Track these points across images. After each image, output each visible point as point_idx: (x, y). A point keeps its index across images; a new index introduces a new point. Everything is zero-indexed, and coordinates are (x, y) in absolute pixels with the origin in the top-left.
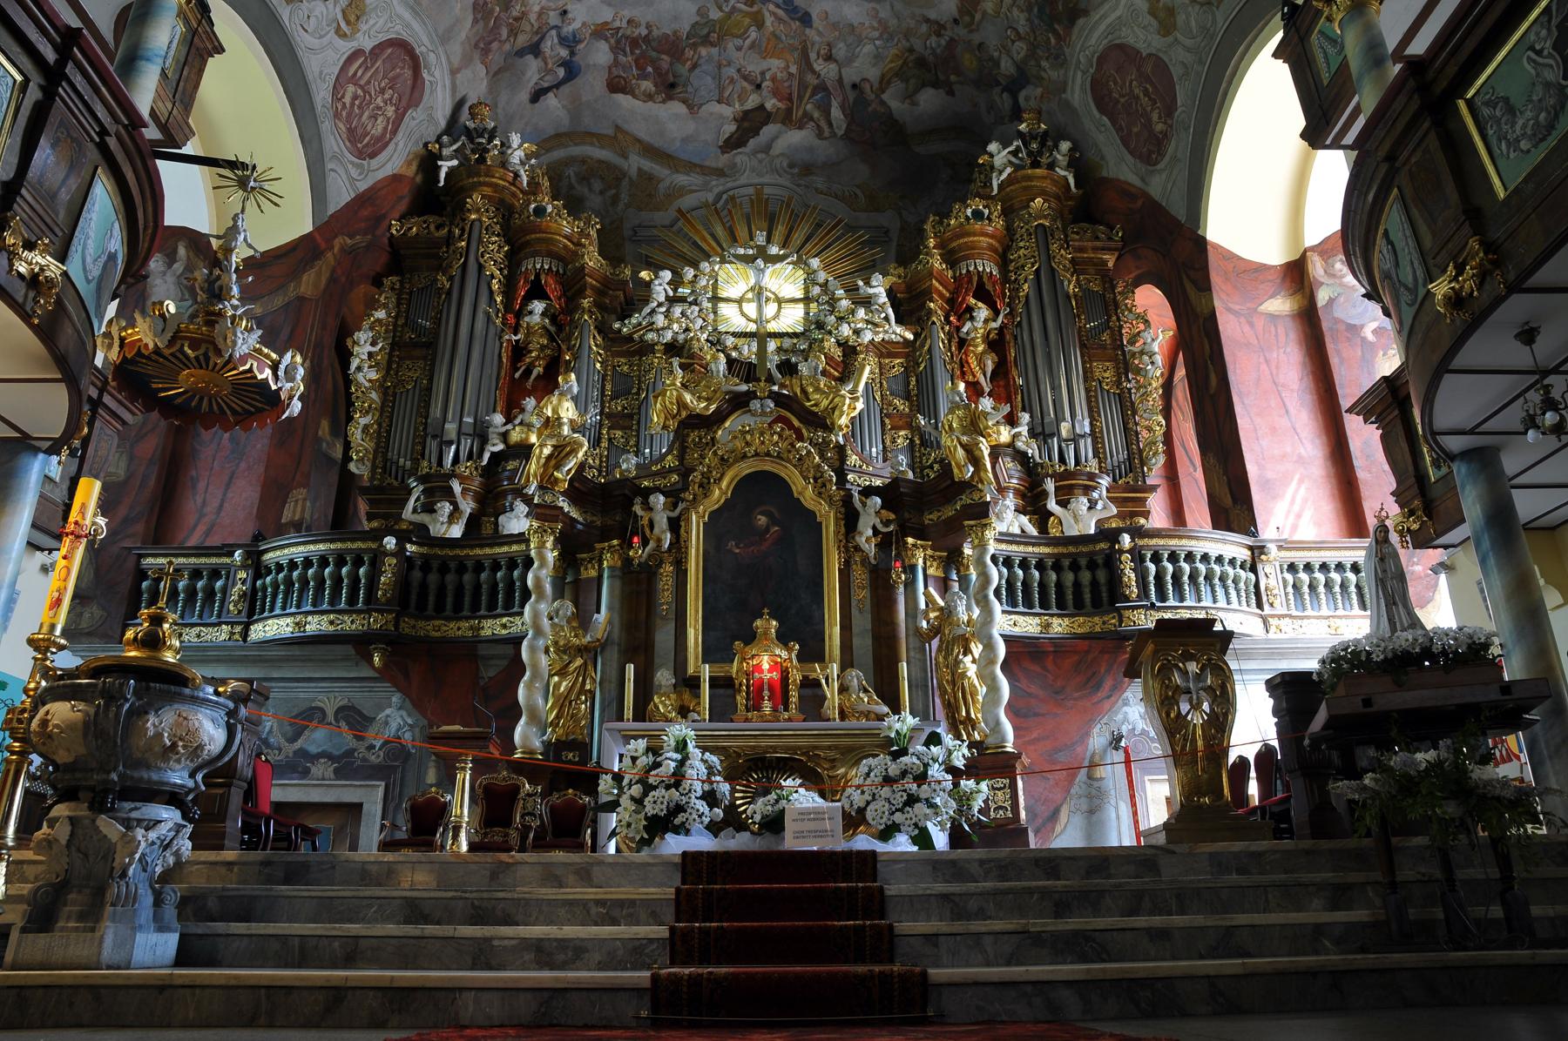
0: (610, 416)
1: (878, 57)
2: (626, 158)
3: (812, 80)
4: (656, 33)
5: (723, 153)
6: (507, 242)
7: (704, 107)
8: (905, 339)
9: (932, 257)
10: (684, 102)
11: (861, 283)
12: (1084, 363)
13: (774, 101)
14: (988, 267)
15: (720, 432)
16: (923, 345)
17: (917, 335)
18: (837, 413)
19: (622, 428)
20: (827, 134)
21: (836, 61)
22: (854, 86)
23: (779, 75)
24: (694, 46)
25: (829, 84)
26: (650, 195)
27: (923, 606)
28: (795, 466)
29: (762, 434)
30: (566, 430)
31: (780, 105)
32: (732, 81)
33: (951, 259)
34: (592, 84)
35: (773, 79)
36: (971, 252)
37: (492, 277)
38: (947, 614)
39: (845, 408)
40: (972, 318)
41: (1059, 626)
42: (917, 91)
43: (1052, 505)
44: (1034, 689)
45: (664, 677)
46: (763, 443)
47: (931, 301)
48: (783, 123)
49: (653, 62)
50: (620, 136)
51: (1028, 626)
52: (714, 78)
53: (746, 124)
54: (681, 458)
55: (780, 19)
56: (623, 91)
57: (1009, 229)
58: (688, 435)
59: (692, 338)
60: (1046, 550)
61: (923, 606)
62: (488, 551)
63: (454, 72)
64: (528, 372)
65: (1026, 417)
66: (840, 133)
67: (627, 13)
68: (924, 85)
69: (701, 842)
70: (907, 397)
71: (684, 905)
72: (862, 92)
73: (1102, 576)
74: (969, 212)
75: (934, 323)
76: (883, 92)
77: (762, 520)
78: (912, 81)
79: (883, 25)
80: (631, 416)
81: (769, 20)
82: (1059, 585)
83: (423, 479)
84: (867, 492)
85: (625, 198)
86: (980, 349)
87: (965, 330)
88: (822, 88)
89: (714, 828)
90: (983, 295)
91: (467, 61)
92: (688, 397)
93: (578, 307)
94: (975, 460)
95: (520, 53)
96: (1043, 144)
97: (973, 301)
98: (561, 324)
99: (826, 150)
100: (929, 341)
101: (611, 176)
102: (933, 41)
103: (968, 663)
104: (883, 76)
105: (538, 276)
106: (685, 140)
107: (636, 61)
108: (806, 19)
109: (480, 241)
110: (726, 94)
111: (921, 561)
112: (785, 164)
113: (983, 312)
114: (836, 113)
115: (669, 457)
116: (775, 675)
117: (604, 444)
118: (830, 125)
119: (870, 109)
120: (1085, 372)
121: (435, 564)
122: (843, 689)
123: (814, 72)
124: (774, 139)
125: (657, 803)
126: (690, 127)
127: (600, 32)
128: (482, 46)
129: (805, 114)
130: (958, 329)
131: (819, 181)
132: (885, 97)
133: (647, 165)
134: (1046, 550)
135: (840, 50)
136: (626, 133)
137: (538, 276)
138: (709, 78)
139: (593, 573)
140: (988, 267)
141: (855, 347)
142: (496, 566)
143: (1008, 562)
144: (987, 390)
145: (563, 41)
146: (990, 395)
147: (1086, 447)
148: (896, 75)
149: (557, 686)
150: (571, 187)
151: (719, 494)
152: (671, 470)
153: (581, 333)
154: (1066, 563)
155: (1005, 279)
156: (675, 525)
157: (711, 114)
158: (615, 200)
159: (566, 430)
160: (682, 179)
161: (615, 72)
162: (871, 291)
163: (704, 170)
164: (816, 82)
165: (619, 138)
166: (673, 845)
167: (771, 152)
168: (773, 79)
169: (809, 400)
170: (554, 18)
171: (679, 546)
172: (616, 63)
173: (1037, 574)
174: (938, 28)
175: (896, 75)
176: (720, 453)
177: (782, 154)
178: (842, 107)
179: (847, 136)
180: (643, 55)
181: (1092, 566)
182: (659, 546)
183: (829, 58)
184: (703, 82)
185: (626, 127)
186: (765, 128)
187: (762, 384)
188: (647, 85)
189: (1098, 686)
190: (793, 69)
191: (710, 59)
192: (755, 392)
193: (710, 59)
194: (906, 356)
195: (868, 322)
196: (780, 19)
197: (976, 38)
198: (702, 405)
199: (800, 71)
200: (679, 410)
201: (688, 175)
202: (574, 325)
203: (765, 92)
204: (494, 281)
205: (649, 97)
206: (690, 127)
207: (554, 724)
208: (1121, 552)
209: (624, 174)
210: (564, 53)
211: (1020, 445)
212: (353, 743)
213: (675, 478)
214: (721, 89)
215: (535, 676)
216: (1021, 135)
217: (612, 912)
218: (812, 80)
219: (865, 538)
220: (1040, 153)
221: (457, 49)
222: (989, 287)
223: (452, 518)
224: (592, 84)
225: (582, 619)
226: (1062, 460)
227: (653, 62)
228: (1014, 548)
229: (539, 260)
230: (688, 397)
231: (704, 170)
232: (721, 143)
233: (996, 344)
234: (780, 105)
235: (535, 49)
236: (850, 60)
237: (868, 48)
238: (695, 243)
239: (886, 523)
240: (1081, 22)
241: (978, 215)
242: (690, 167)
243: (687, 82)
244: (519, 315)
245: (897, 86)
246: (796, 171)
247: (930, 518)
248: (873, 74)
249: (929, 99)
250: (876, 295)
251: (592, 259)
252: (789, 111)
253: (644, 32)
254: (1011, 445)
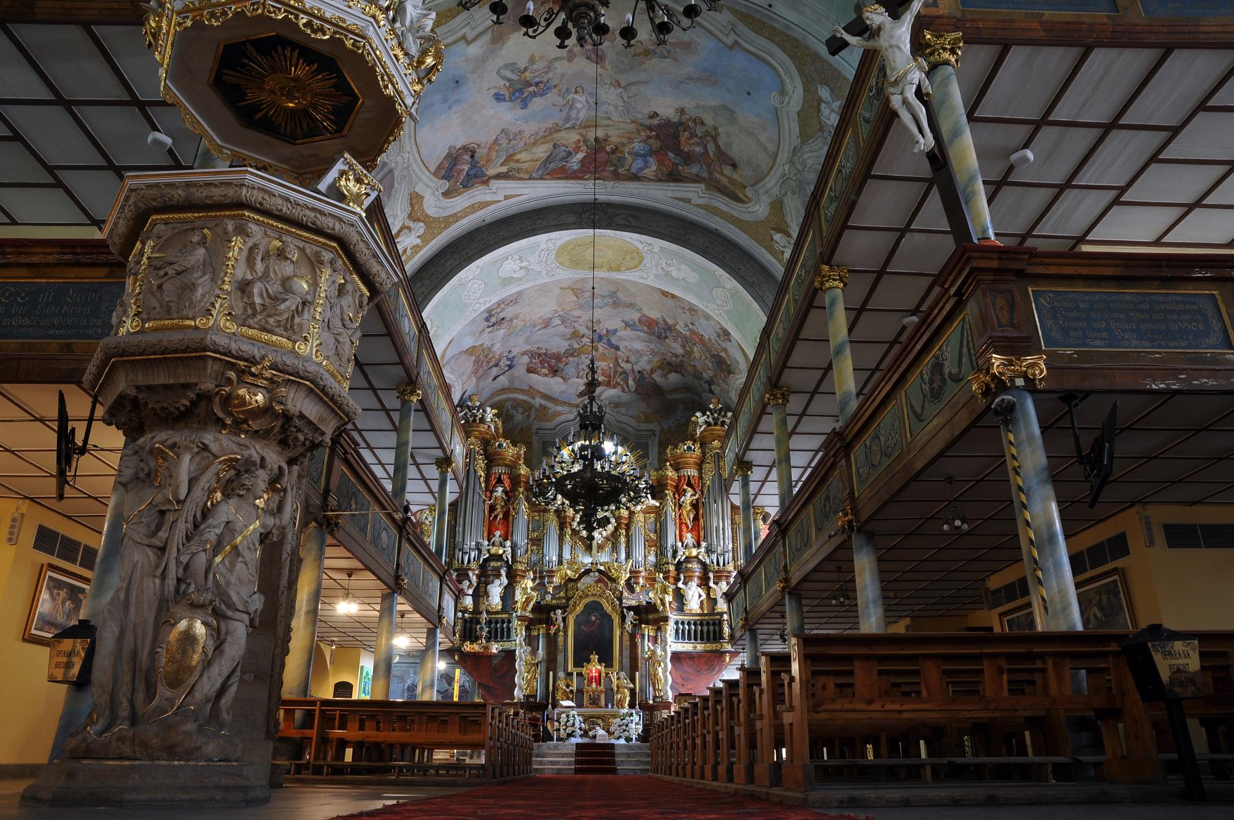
0: (532, 540)
1: (650, 362)
2: (534, 399)
3: (620, 370)
4: (549, 352)
6: (487, 458)
8: (656, 507)
12: (732, 515)
14: (692, 472)
16: (663, 508)
17: (661, 504)
19: (537, 545)
20: (626, 389)
22: (639, 372)
24: (567, 357)
25: (628, 371)
26: (545, 415)
27: (647, 650)
30: (529, 591)
32: (583, 370)
33: (677, 468)
34: (520, 370)
35: (602, 369)
36: (686, 465)
37: (481, 476)
38: (654, 652)
40: (685, 495)
41: (700, 647)
42: (668, 374)
43: (711, 584)
44: (689, 670)
45: (561, 674)
49: (548, 362)
50: (531, 390)
51: (687, 647)
54: (566, 593)
55: (605, 348)
56: (534, 372)
57: (704, 454)
60: (698, 618)
61: (647, 650)
62: (493, 616)
63: (463, 384)
64: (496, 517)
65: (704, 544)
67: (537, 346)
68: (671, 372)
69: (579, 740)
70: (656, 532)
71: (577, 754)
72: (643, 374)
73: (717, 628)
74: (685, 447)
77: (594, 618)
78: (666, 370)
79: (653, 352)
80: (540, 540)
81: (600, 349)
82: (702, 631)
83: (456, 570)
84: (630, 608)
85: (533, 416)
86: (689, 508)
87: (682, 500)
88: (625, 372)
89: (581, 736)
90: (689, 485)
91: (469, 378)
92: (569, 572)
93: (517, 490)
94: (663, 604)
95: (490, 368)
96: (719, 414)
97: (686, 487)
98: (510, 496)
99: (626, 397)
101: (527, 407)
102: (674, 359)
103: (660, 670)
105: (500, 476)
106: (561, 392)
107: (540, 362)
108: (617, 348)
109: (475, 459)
111: (647, 633)
112: (607, 403)
113: (690, 491)
114: (631, 382)
116: (597, 674)
117: (529, 552)
118: (628, 387)
120: (732, 520)
121: (474, 620)
122: (618, 678)
125: (569, 730)
126: (564, 387)
127: (524, 353)
128: (475, 372)
129: (617, 382)
130: (679, 500)
131: (623, 410)
132: (653, 376)
133: (543, 402)
134: (698, 618)
135: (633, 359)
136: (534, 389)
137: (500, 476)
139: (536, 634)
140: (692, 472)
142: (497, 622)
143: (683, 623)
144: (690, 527)
145: (508, 359)
146: (691, 532)
147: (729, 556)
148: (658, 368)
149: (527, 676)
150: (508, 411)
151: (579, 609)
152: (563, 598)
153: (519, 503)
154: (705, 623)
155: (701, 478)
156: (564, 619)
158: (528, 417)
159: (529, 591)
160: (559, 408)
161: (530, 365)
163: (570, 405)
165: (531, 391)
166: (574, 741)
168: (602, 369)
170: (505, 354)
171: (565, 627)
172: (531, 362)
173: (693, 627)
174: (677, 356)
175: (658, 368)
178: (634, 380)
179: (636, 391)
180: (543, 359)
181: (714, 624)
182: (559, 628)
183: (628, 362)
184: (570, 370)
185: (534, 386)
188: (545, 371)
189: (713, 669)
190: (611, 366)
191: (573, 362)
193: (573, 362)
194: (656, 513)
196: (605, 348)
197: (693, 363)
199: (614, 367)
202: (516, 498)
204: (482, 478)
205: (546, 375)
206: (564, 387)
207: (526, 689)
208: (724, 620)
209: (533, 406)
210: (509, 363)
211: (700, 557)
212: (448, 687)
213: (564, 601)
214: (578, 373)
215: (520, 674)
216: (710, 410)
217: (564, 755)
218: (620, 370)
219: (628, 626)
220: (718, 419)
221: (465, 377)
222: (693, 482)
223: (469, 587)
224: (520, 370)
225: (534, 652)
226: (718, 564)
227: (548, 362)
228: (686, 617)
229: (500, 468)
230: (568, 572)
231: (570, 405)
233: (695, 506)
235: (496, 365)
236: (637, 363)
237: (645, 358)
239: (635, 620)
240: (732, 375)
241: (689, 448)
242: (564, 403)
243: (563, 370)
244: (492, 492)
245: (659, 372)
247: (651, 616)
248: (648, 368)
249: (673, 377)
251: (523, 470)
252: (609, 381)
253: (544, 351)
254: (696, 557)
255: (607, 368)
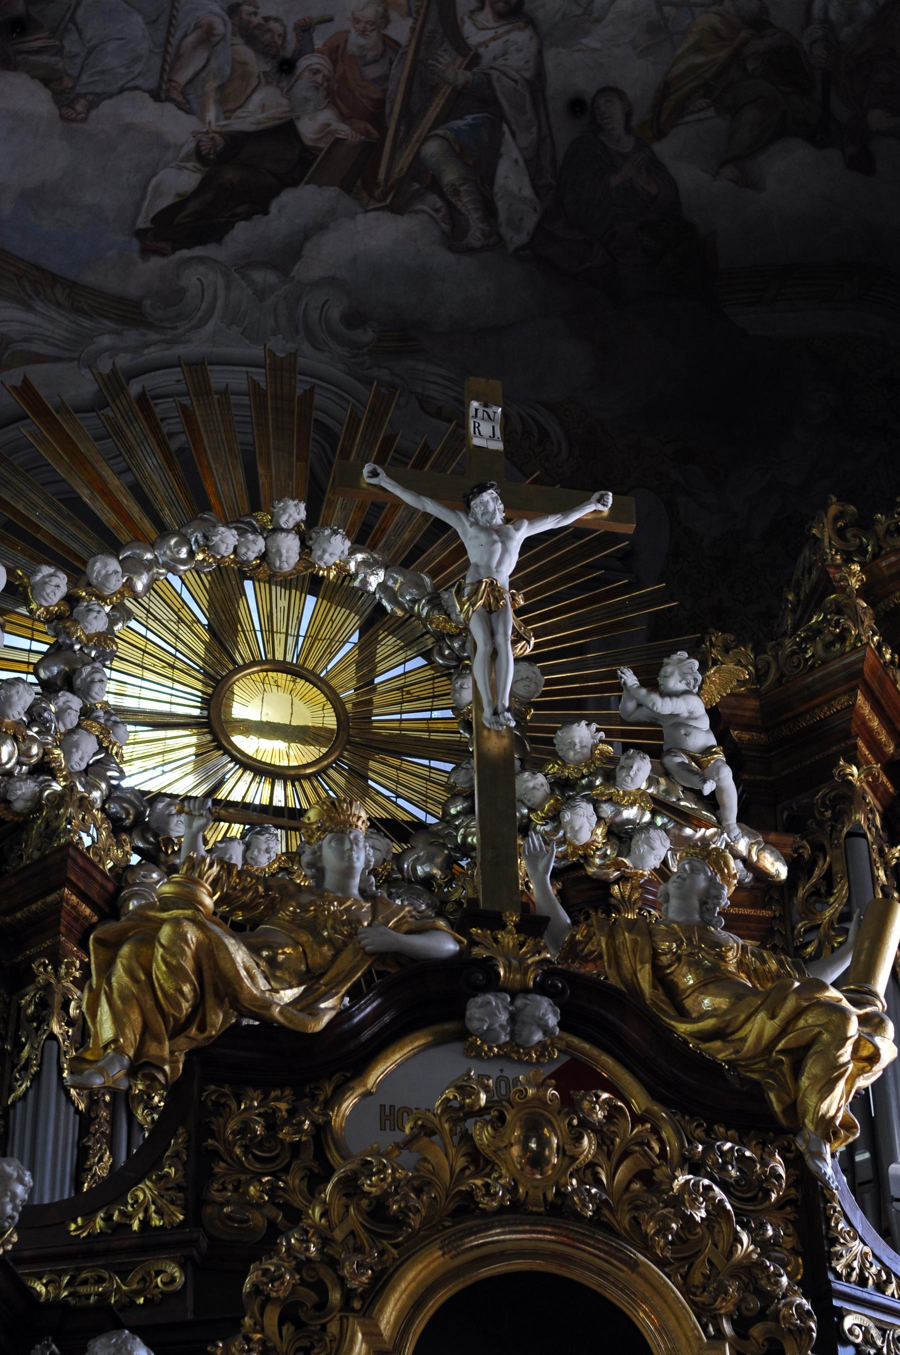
5: (146, 252)
7: (106, 106)
9: (858, 622)
10: (46, 82)
11: (630, 678)
13: (327, 116)
15: (349, 1104)
18: (812, 1068)
20: (475, 233)
21: (531, 23)
23: (355, 39)
28: (661, 1263)
29: (533, 1128)
31: (344, 130)
32: (208, 37)
39: (846, 1054)
46: (537, 1161)
47: (853, 760)
48: (347, 186)
52: (152, 23)
53: (230, 175)
58: (219, 1108)
59: (60, 800)
66: (517, 239)
75: (857, 833)
76: (661, 135)
100: (842, 890)
104: (666, 88)
110: (183, 77)
112: (335, 313)
115: (144, 1191)
118: (489, 210)
119: (614, 181)
123: (460, 45)
124: (318, 228)
132: (664, 149)
138: (137, 19)
141: (604, 885)
157: (128, 128)
162: (665, 706)
164: (464, 77)
167: (299, 271)
169: (683, 1014)
176: (370, 1185)
177: (331, 281)
186: (288, 197)
187: (508, 939)
192: (488, 966)
195: (659, 806)
198: (288, 995)
200: (199, 1005)
201: (30, 308)
203: (303, 87)
232: (142, 222)
234: (344, 130)
238: (74, 503)
246: (367, 336)
250: (678, 722)
255: (372, 39)
